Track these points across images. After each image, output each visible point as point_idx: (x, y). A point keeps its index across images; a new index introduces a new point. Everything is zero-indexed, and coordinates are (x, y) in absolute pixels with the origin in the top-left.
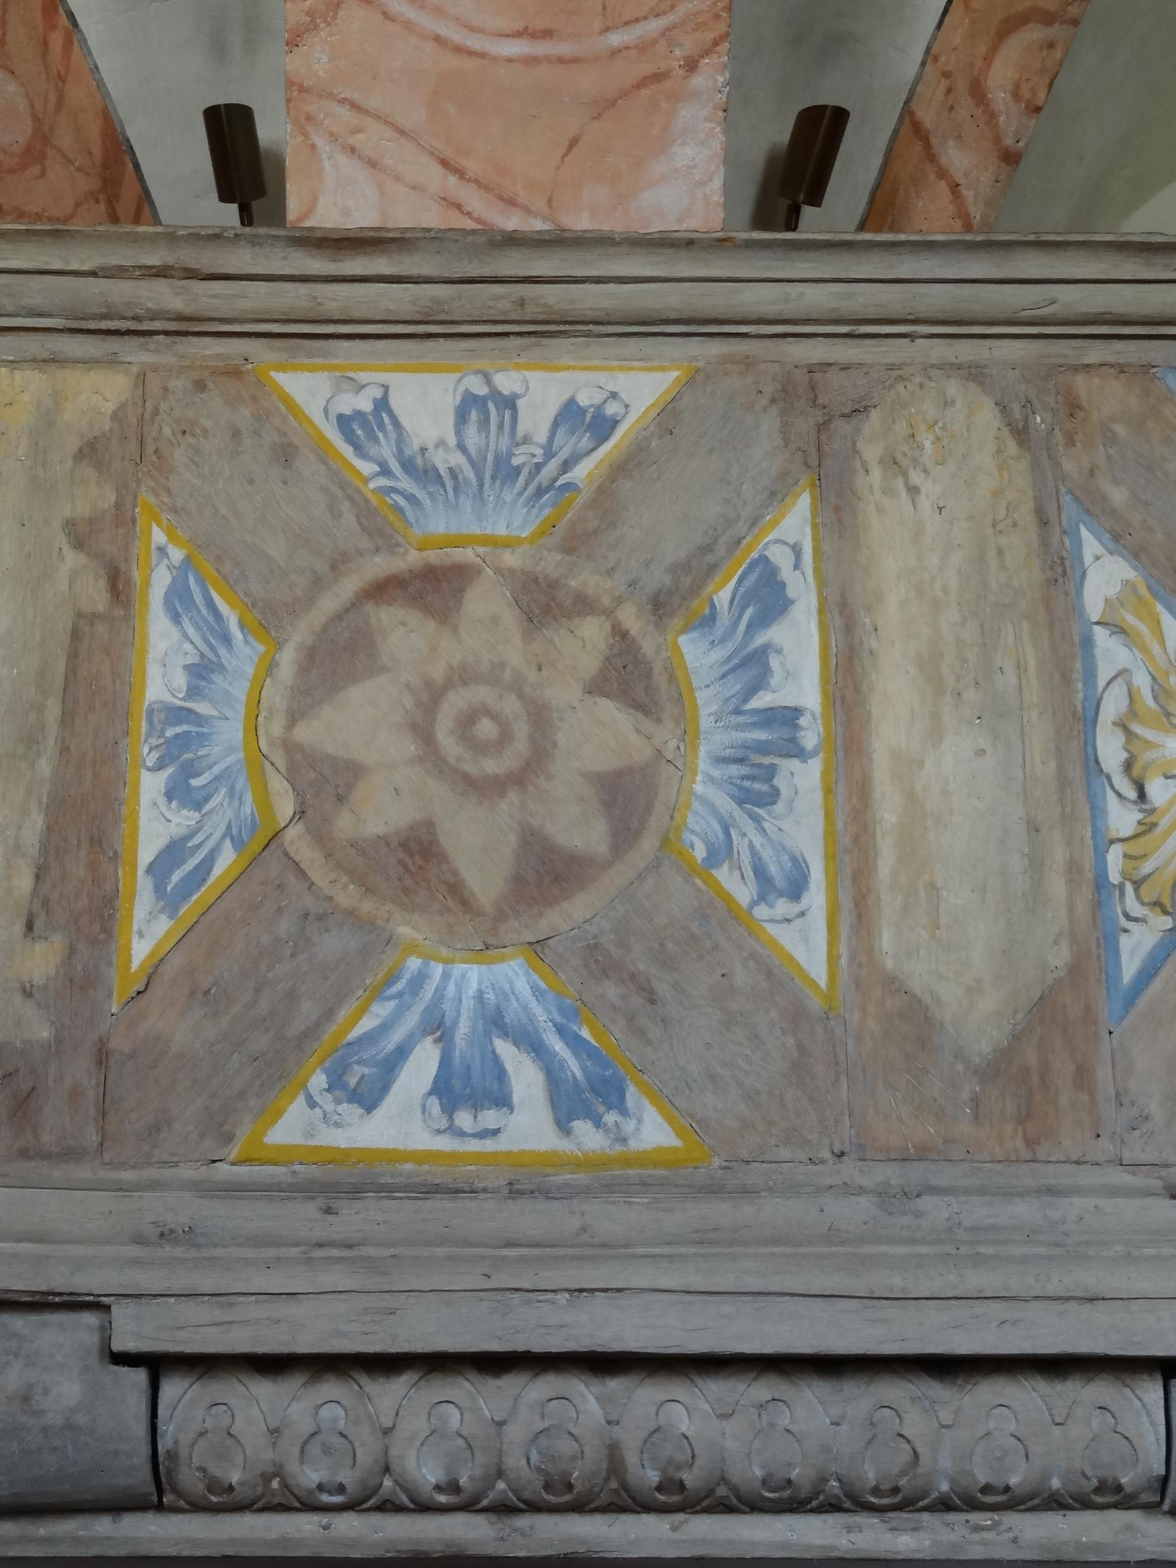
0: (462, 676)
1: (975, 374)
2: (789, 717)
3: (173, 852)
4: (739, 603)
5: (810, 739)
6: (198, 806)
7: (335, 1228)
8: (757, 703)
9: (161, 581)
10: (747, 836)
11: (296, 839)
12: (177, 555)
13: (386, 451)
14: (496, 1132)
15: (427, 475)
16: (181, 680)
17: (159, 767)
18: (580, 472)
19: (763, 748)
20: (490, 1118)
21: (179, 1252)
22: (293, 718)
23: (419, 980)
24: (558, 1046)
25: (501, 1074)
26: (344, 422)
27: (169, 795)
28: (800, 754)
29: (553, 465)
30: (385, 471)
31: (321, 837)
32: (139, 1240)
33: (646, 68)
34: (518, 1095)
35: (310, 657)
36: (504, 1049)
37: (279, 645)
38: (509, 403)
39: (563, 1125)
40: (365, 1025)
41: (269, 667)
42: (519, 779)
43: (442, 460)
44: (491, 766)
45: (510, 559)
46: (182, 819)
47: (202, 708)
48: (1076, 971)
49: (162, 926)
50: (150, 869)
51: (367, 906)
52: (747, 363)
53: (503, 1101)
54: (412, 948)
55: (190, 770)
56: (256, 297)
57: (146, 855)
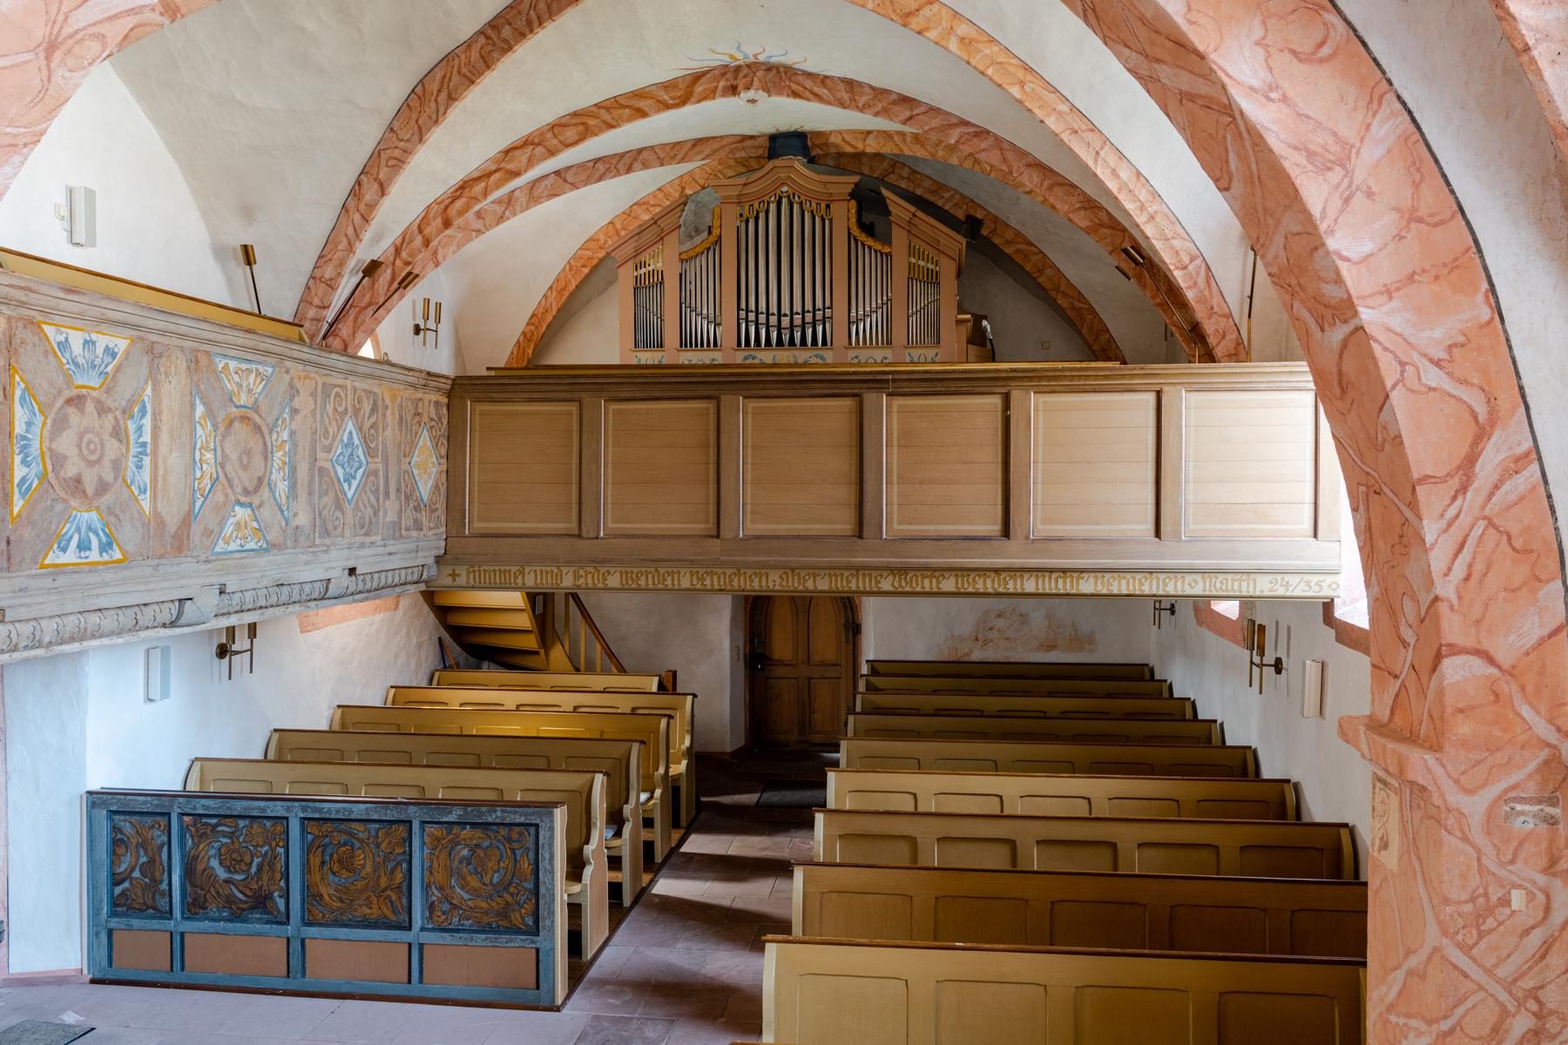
0: (87, 431)
1: (182, 349)
2: (144, 445)
3: (23, 480)
4: (139, 411)
5: (148, 451)
6: (29, 466)
7: (57, 584)
8: (140, 440)
9: (18, 393)
10: (137, 478)
11: (51, 476)
12: (23, 385)
13: (68, 357)
14: (87, 557)
15: (77, 365)
16: (24, 427)
17: (19, 454)
18: (109, 369)
19: (141, 453)
20: (87, 553)
21: (21, 593)
22: (51, 440)
23: (76, 517)
24: (101, 533)
25: (90, 542)
26: (59, 344)
27: (22, 463)
28: (147, 455)
29: (103, 366)
30: (68, 363)
31: (57, 478)
32: (14, 592)
33: (13, 142)
34: (93, 547)
35: (54, 422)
36: (91, 534)
37: (46, 417)
38: (94, 343)
39: (101, 555)
40: (65, 530)
41: (44, 424)
42: (98, 461)
43: (81, 360)
44: (94, 458)
45: (94, 394)
46: (26, 470)
47: (29, 436)
48: (189, 511)
49: (21, 503)
50: (18, 485)
51: (66, 497)
52: (141, 339)
53: (90, 549)
54: (74, 509)
55: (26, 456)
56: (44, 301)
57: (16, 481)
